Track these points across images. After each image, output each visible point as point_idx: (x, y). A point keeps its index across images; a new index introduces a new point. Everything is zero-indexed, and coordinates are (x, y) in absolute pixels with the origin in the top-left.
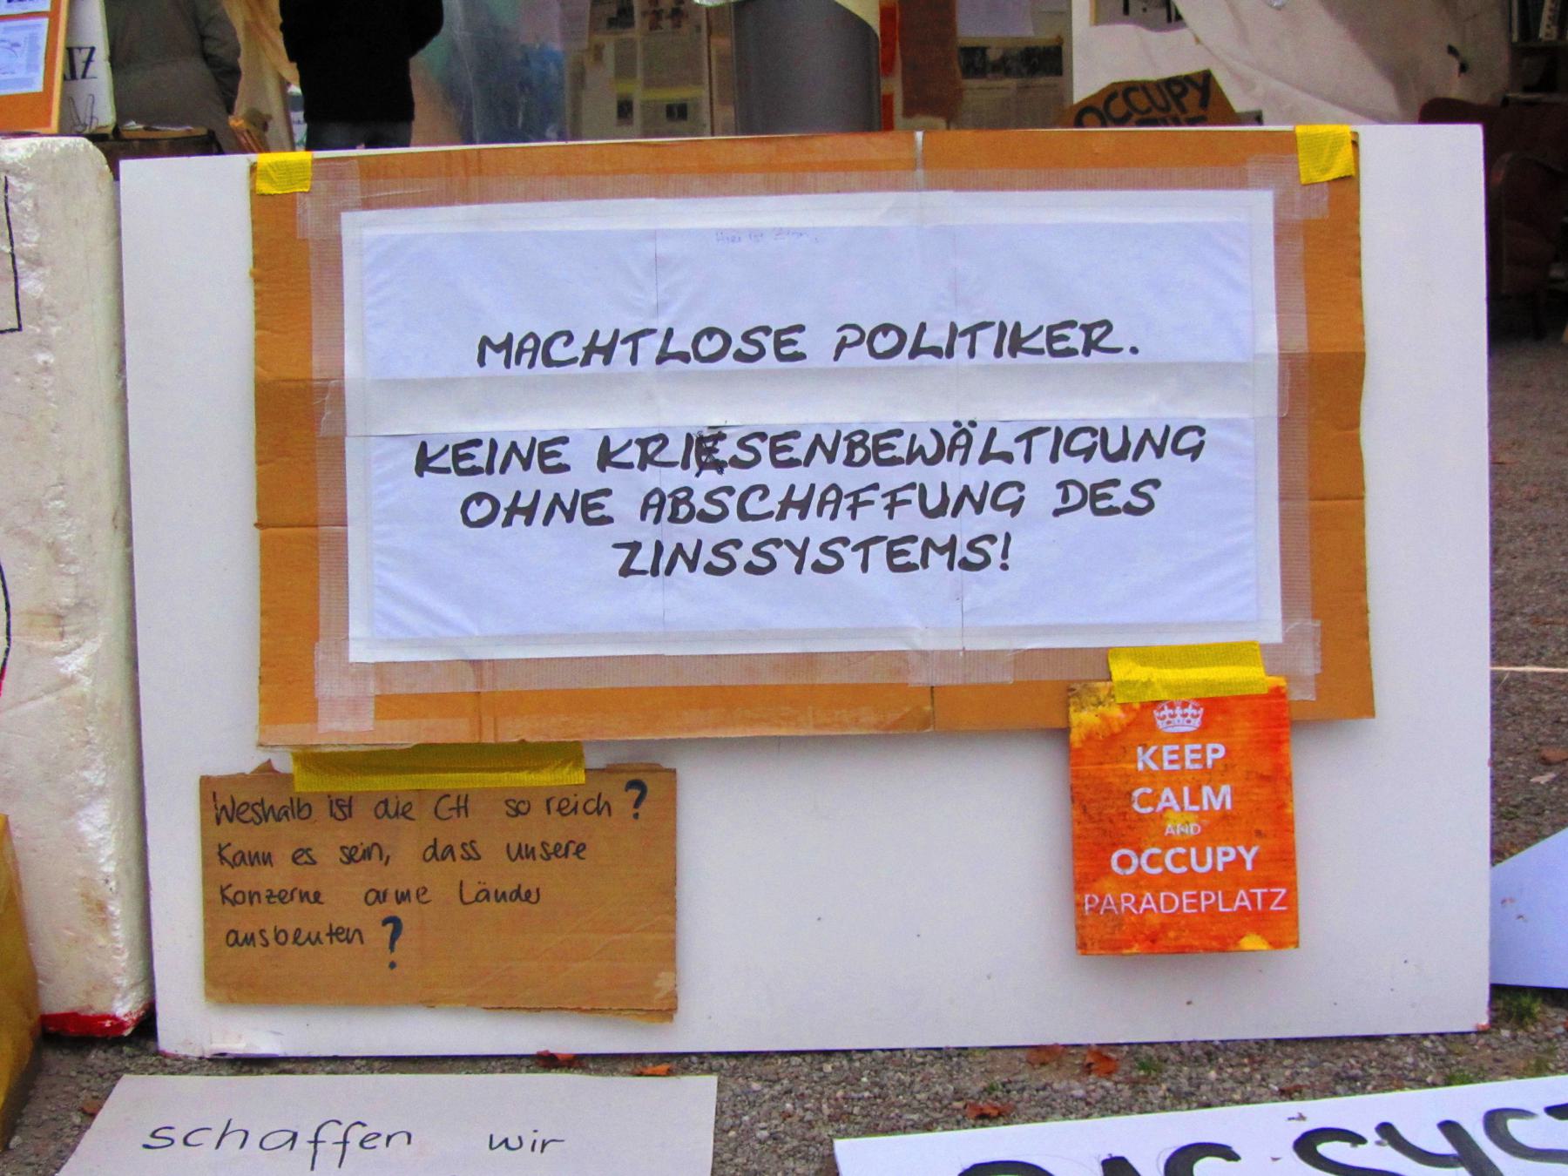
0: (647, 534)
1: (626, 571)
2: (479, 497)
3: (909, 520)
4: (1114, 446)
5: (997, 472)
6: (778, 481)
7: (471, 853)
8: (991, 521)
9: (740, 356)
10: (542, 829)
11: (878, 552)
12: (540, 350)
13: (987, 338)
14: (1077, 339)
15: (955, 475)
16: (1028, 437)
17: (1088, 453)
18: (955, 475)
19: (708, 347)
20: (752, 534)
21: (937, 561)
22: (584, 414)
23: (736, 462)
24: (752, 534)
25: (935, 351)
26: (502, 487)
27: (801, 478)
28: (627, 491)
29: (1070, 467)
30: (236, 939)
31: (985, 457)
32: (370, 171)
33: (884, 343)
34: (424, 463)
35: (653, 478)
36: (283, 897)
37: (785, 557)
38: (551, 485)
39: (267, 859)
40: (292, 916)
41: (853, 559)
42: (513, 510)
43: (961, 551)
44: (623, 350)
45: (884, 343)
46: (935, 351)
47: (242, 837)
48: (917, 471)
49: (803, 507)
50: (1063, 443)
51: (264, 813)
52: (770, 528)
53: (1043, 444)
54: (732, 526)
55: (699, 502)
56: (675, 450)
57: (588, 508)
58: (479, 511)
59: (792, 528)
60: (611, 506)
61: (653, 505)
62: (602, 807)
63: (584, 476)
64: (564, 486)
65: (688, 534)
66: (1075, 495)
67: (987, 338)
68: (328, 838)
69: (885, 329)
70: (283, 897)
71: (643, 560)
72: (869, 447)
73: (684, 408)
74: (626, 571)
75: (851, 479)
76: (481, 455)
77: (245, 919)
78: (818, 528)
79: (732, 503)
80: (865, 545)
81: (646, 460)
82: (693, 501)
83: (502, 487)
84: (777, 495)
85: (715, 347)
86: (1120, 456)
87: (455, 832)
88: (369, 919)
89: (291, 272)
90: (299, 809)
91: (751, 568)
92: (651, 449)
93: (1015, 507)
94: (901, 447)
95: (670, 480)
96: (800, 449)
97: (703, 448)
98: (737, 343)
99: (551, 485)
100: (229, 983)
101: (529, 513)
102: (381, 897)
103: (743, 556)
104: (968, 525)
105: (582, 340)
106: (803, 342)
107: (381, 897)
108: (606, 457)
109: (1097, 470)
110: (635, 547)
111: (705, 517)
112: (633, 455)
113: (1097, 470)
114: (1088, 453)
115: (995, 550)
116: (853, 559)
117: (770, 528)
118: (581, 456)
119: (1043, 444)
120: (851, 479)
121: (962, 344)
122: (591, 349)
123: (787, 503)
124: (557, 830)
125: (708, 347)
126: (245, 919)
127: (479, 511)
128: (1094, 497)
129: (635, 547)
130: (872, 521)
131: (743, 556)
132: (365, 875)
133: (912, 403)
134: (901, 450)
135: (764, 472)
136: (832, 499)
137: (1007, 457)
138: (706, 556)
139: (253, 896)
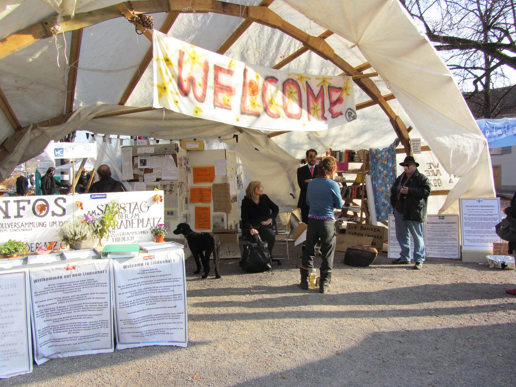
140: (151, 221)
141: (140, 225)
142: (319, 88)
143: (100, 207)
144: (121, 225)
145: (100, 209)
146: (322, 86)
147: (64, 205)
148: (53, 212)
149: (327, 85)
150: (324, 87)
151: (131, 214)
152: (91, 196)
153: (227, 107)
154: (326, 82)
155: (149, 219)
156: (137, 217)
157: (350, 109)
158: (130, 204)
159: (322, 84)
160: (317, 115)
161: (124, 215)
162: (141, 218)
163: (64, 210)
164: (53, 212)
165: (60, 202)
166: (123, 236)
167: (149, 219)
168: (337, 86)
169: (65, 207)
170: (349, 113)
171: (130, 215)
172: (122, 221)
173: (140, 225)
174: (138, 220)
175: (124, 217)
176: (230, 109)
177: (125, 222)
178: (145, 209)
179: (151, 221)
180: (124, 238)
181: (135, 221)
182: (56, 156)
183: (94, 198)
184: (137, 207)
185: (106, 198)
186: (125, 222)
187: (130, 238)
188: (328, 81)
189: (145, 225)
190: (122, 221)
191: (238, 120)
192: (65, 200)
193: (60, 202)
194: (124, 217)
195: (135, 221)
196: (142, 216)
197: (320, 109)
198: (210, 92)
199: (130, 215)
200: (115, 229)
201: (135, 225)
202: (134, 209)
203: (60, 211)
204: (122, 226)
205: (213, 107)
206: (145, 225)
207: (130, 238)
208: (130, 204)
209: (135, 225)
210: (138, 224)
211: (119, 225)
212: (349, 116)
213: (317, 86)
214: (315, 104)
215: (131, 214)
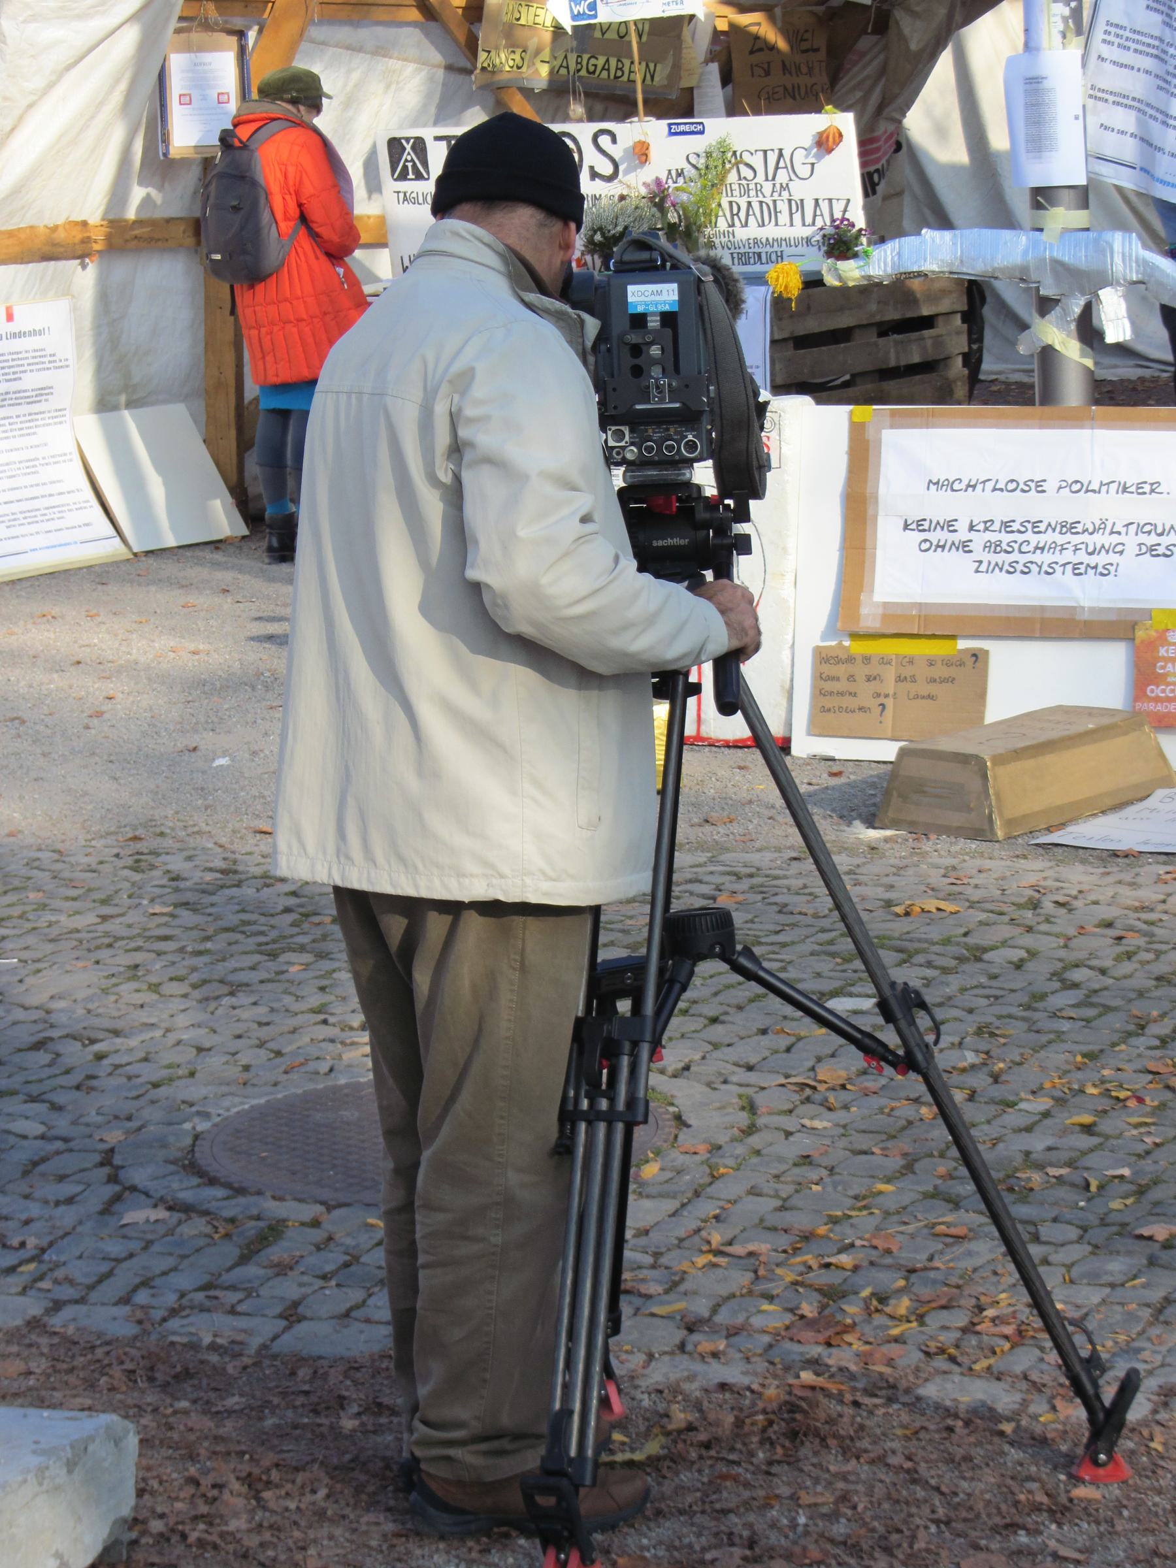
0: (986, 557)
1: (977, 571)
2: (925, 541)
3: (1081, 556)
4: (1159, 530)
5: (1115, 539)
6: (1034, 539)
7: (913, 680)
8: (1113, 558)
9: (1023, 491)
10: (940, 671)
11: (1069, 568)
12: (950, 485)
13: (1114, 487)
14: (1147, 488)
15: (1099, 539)
16: (1127, 525)
17: (1149, 533)
18: (1099, 539)
19: (1011, 486)
20: (1023, 559)
21: (1091, 572)
22: (963, 508)
23: (1019, 532)
24: (1023, 559)
25: (1094, 491)
26: (936, 536)
27: (1042, 539)
28: (978, 540)
29: (1143, 538)
30: (825, 710)
31: (1112, 533)
32: (893, 414)
33: (1076, 487)
34: (906, 527)
35: (989, 536)
36: (841, 694)
37: (1034, 568)
38: (952, 537)
39: (838, 679)
40: (846, 701)
41: (1059, 570)
42: (938, 546)
43: (1100, 569)
44: (979, 487)
45: (1076, 487)
46: (1094, 491)
47: (828, 669)
48: (1085, 537)
49: (1042, 549)
50: (1140, 529)
51: (838, 661)
52: (1030, 557)
53: (1133, 528)
54: (1015, 556)
55: (1004, 546)
56: (996, 526)
57: (965, 547)
58: (925, 546)
59: (1038, 557)
60: (972, 546)
61: (988, 546)
62: (962, 664)
63: (963, 534)
64: (956, 537)
65: (1001, 558)
66: (1144, 549)
67: (1114, 487)
68: (861, 671)
69: (1077, 482)
70: (841, 694)
71: (983, 568)
72: (1069, 527)
73: (1002, 507)
74: (977, 571)
75: (1060, 539)
76: (926, 525)
77: (829, 702)
78: (1046, 558)
79: (1016, 546)
80: (1064, 565)
81: (986, 529)
82: (1006, 545)
83: (936, 536)
84: (1033, 545)
85: (1013, 486)
86: (1161, 534)
87: (908, 671)
88: (873, 703)
89: (862, 456)
90: (851, 660)
91: (1023, 572)
92: (988, 524)
93: (1121, 552)
94: (1080, 528)
95: (993, 537)
96: (1042, 527)
97: (1006, 525)
98: (1022, 486)
99: (952, 537)
100: (818, 728)
101: (943, 547)
102: (879, 695)
103: (1019, 567)
104: (1101, 559)
105: (965, 482)
106: (1045, 486)
107: (879, 695)
108: (971, 528)
109: (1152, 539)
110: (981, 562)
111: (1007, 552)
112: (981, 527)
113: (1152, 539)
114: (1149, 533)
115: (1112, 569)
116: (1059, 570)
117: (1030, 557)
118: (962, 526)
119: (1133, 528)
120: (1060, 539)
121: (1104, 489)
122: (969, 486)
123: (1037, 548)
124: (945, 672)
125: (1011, 486)
126: (829, 702)
127: (925, 546)
128: (1151, 549)
129: (981, 562)
130: (1068, 556)
131: (1019, 567)
132: (873, 686)
133: (1088, 510)
134: (1080, 529)
135: (1029, 536)
136: (1053, 546)
137: (1119, 533)
138: (1006, 567)
139: (831, 693)
140: (824, 206)
141: (797, 217)
143: (693, 160)
144: (748, 215)
145: (694, 166)
147: (616, 151)
148: (592, 168)
151: (770, 184)
152: (670, 125)
155: (817, 201)
156: (785, 194)
158: (765, 152)
161: (752, 186)
162: (796, 197)
163: (616, 166)
164: (592, 168)
165: (604, 141)
166: (757, 250)
167: (817, 201)
169: (617, 158)
171: (767, 187)
172: (749, 203)
173: (797, 217)
174: (790, 201)
175: (752, 193)
177: (756, 206)
178: (804, 171)
179: (824, 206)
180: (759, 255)
181: (783, 206)
182: (574, 17)
183: (676, 134)
184: (782, 164)
185: (702, 132)
186: (756, 206)
187: (774, 257)
189: (809, 220)
190: (749, 203)
192: (614, 141)
193: (604, 141)
194: (752, 193)
195: (783, 206)
196: (798, 190)
199: (767, 187)
200: (733, 225)
201: (784, 218)
202: (777, 168)
203: (606, 168)
204: (751, 218)
206: (809, 220)
207: (774, 257)
208: (765, 152)
209: (784, 218)
210: (791, 214)
211: (742, 215)
215: (770, 184)
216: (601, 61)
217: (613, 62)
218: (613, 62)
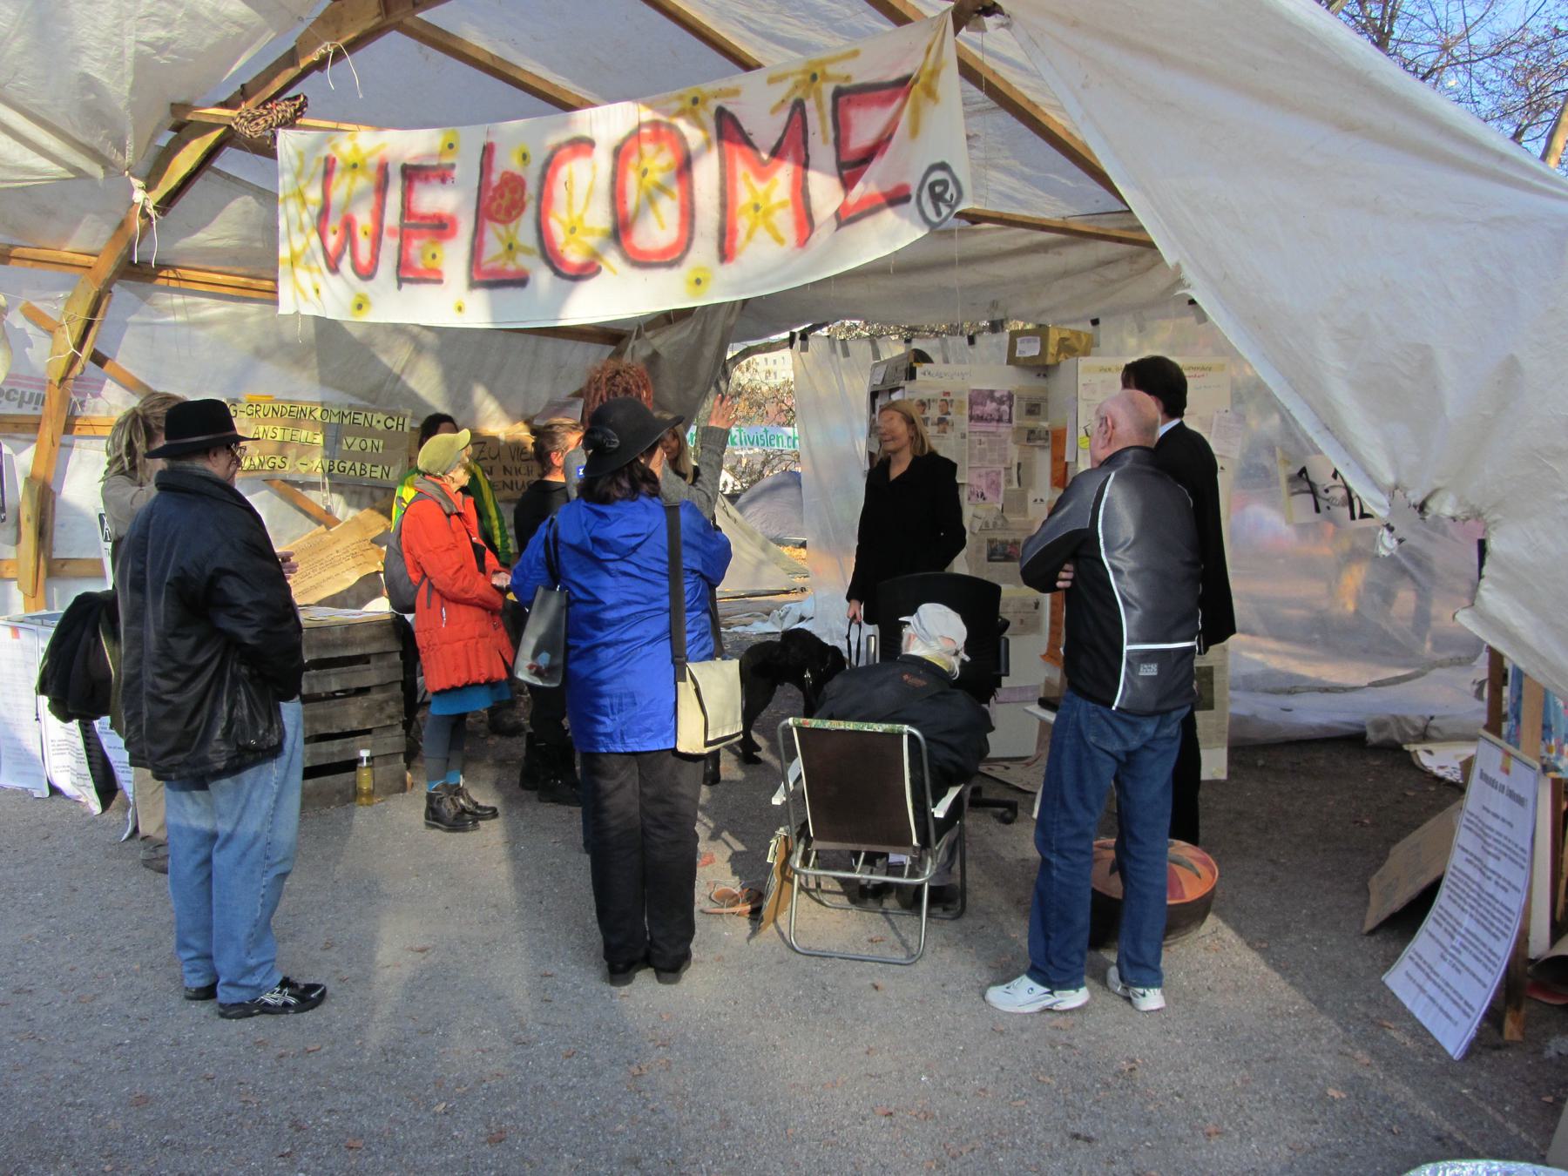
142: (784, 116)
146: (799, 106)
149: (828, 89)
150: (810, 104)
153: (432, 277)
154: (826, 78)
157: (943, 166)
159: (799, 94)
160: (771, 229)
168: (894, 76)
170: (932, 186)
176: (440, 281)
188: (831, 70)
191: (460, 309)
197: (782, 205)
198: (390, 245)
205: (395, 283)
212: (937, 198)
213: (775, 110)
214: (761, 187)
216: (348, 465)
217: (358, 466)
218: (358, 466)
